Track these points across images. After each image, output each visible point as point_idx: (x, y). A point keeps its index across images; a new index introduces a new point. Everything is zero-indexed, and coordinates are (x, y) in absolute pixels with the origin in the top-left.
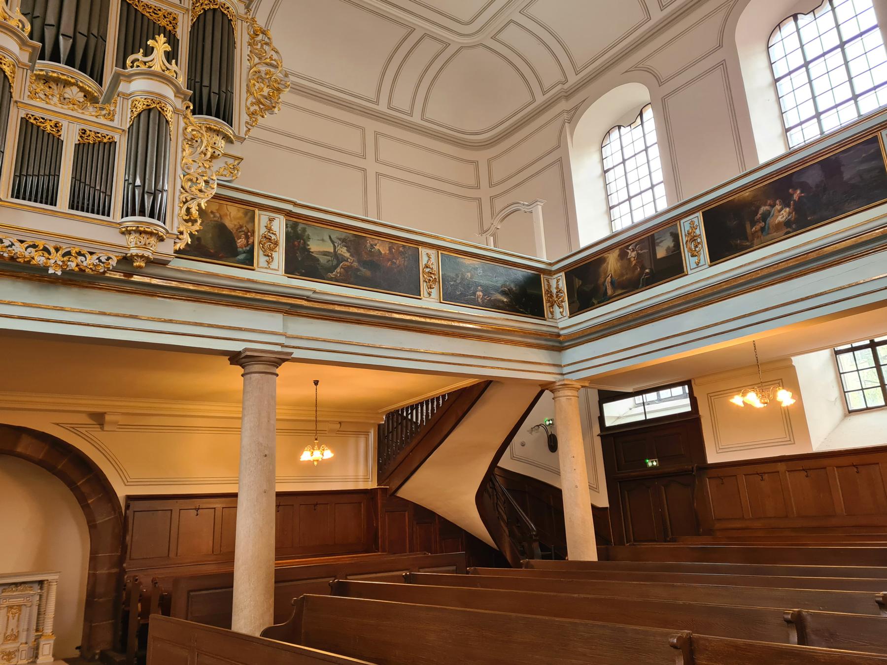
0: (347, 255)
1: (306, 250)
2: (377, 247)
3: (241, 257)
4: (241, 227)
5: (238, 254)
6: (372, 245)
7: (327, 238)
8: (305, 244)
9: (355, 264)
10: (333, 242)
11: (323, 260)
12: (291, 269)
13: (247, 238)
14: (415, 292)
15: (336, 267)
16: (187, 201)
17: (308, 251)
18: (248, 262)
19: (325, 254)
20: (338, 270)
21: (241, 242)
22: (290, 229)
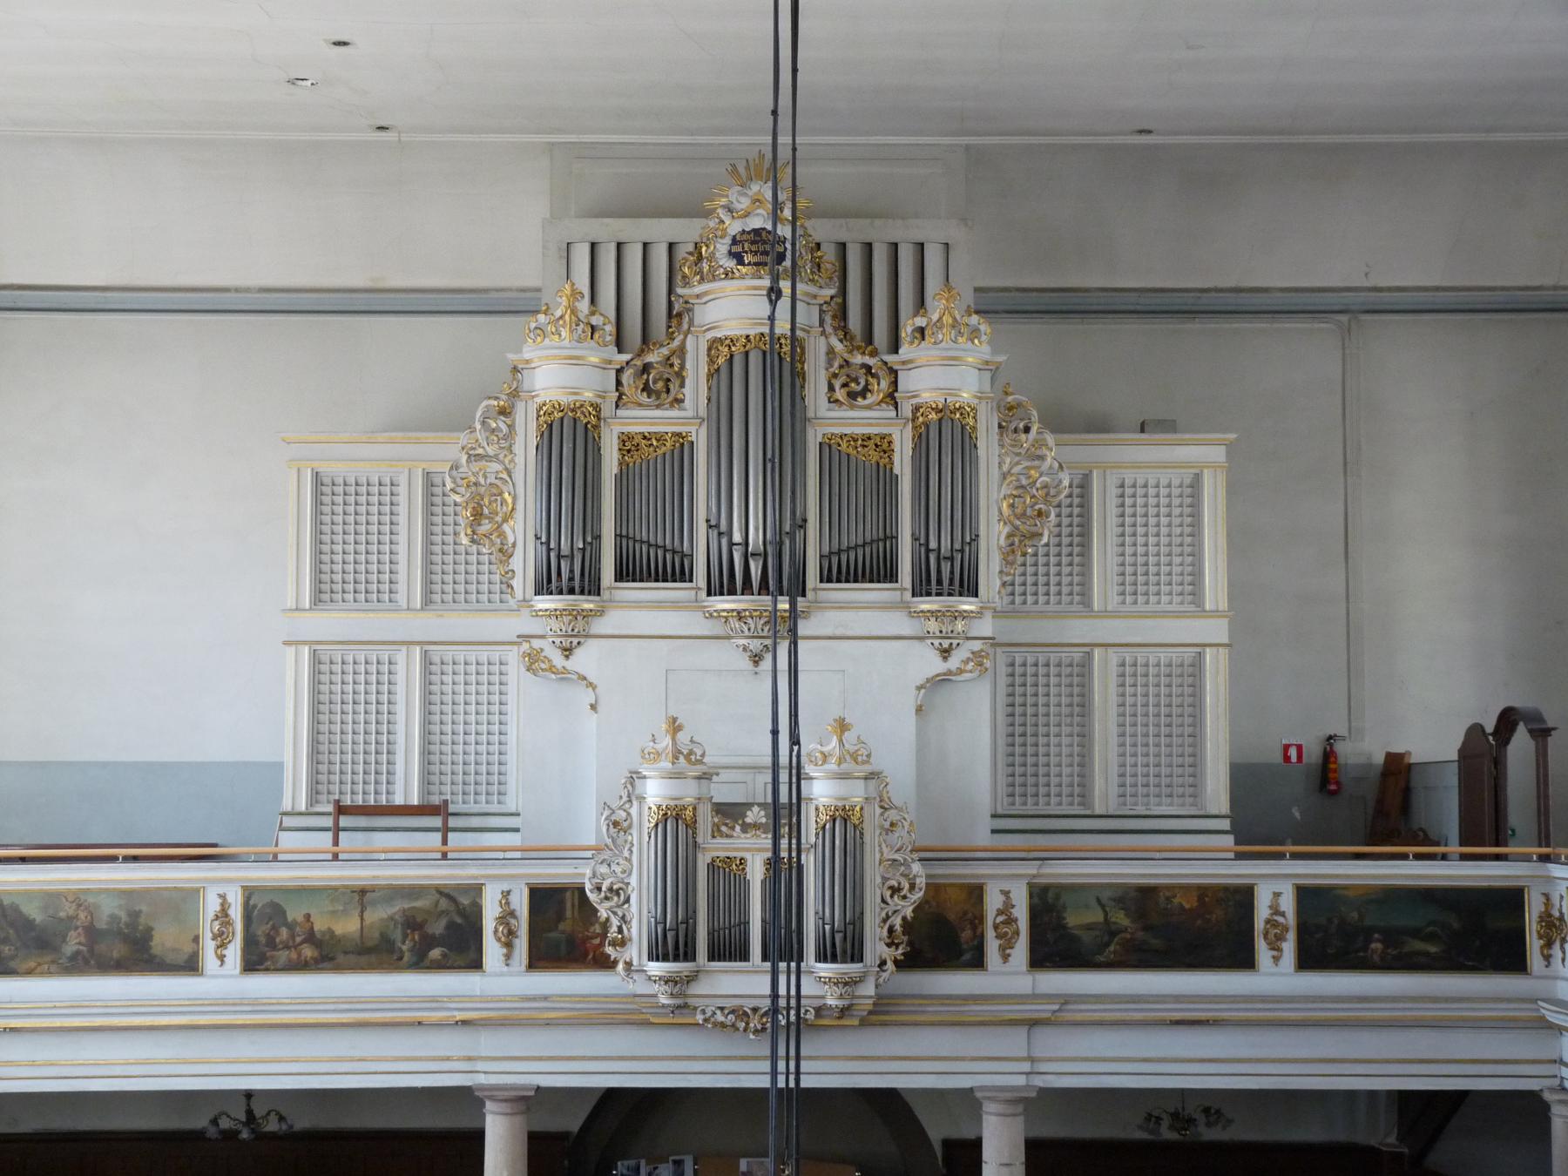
0: (1126, 922)
1: (1061, 926)
2: (1176, 901)
3: (967, 957)
4: (965, 913)
5: (961, 953)
6: (1168, 899)
7: (1093, 903)
8: (1061, 918)
9: (1140, 935)
10: (1103, 906)
11: (1087, 937)
12: (1041, 959)
13: (974, 928)
14: (1243, 959)
15: (1108, 945)
16: (888, 917)
17: (1064, 927)
18: (977, 962)
19: (1089, 927)
20: (1112, 948)
21: (966, 934)
22: (1036, 900)
